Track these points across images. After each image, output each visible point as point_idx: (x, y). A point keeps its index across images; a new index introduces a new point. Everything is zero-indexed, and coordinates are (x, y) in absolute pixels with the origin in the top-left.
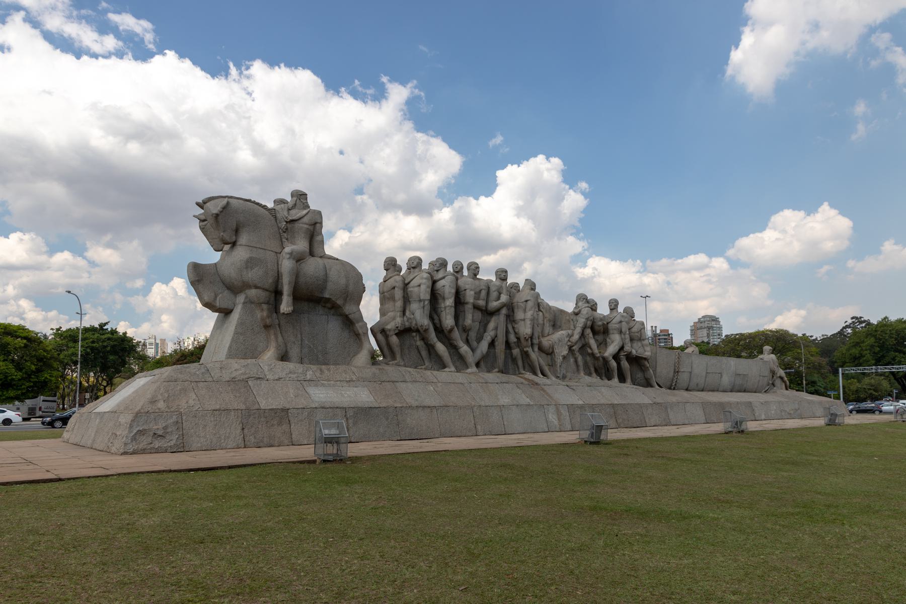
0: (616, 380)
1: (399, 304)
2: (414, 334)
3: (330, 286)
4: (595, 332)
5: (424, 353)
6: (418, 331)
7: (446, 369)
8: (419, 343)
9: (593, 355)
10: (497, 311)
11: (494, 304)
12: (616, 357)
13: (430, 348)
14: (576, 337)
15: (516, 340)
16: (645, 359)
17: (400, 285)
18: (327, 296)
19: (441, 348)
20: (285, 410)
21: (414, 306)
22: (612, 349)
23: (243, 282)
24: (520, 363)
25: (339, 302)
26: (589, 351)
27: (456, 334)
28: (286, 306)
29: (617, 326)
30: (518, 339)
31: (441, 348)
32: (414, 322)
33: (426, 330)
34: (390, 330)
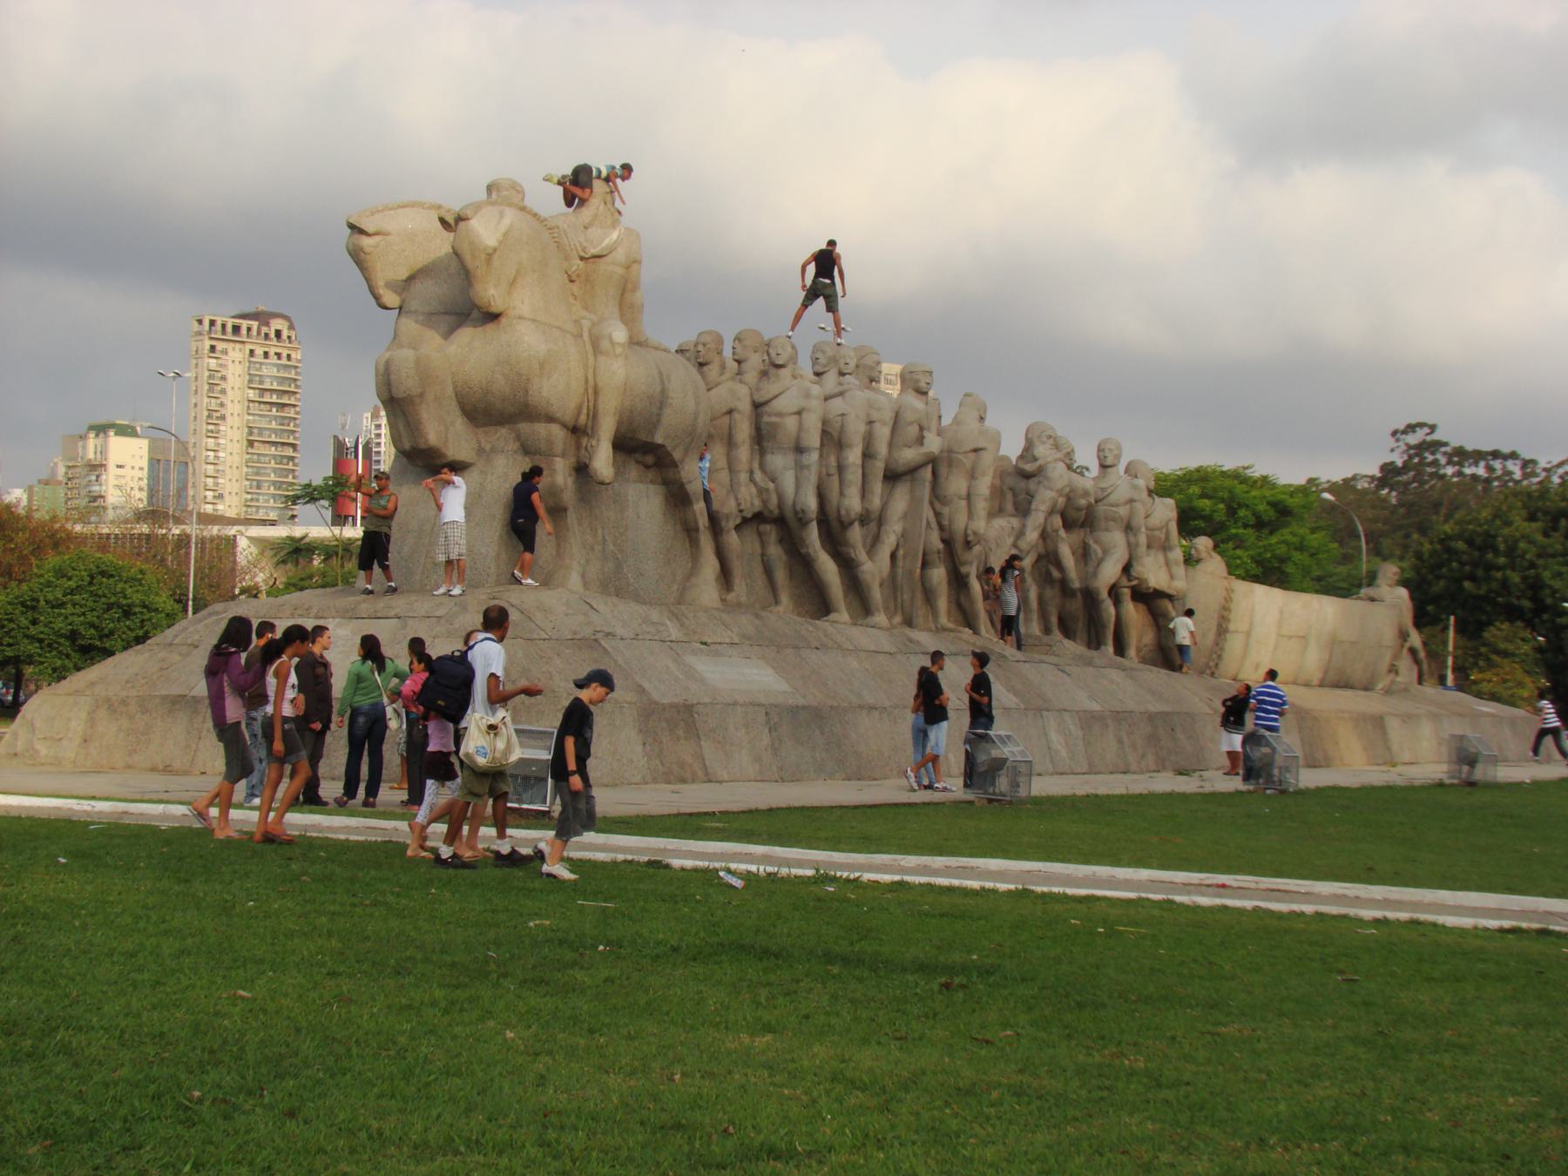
0: (1110, 649)
1: (744, 453)
2: (767, 528)
3: (670, 418)
4: (1068, 525)
5: (781, 575)
6: (780, 521)
7: (833, 616)
8: (775, 551)
9: (1064, 585)
10: (912, 471)
11: (909, 455)
12: (1114, 591)
13: (802, 564)
14: (1032, 536)
15: (941, 546)
16: (1170, 597)
17: (745, 406)
18: (659, 439)
19: (828, 567)
20: (689, 708)
21: (780, 461)
22: (1110, 572)
23: (527, 405)
24: (943, 603)
25: (677, 455)
26: (1056, 574)
27: (856, 534)
28: (603, 461)
29: (1123, 511)
30: (948, 542)
31: (828, 567)
32: (774, 500)
33: (803, 522)
34: (728, 517)
